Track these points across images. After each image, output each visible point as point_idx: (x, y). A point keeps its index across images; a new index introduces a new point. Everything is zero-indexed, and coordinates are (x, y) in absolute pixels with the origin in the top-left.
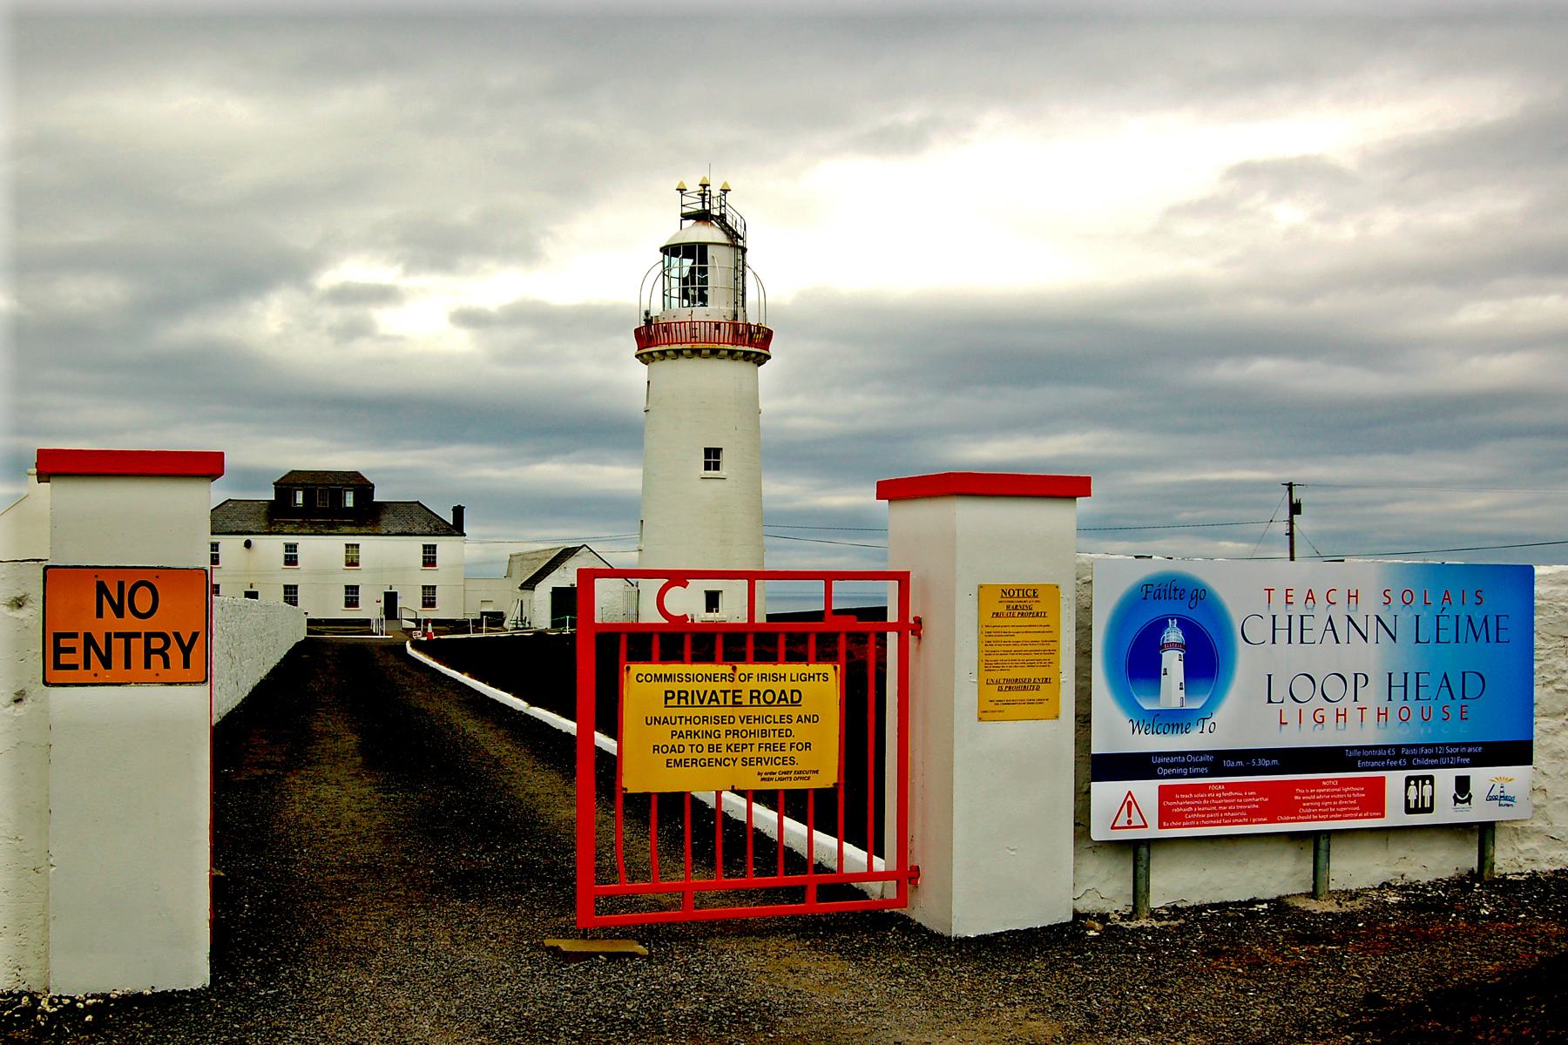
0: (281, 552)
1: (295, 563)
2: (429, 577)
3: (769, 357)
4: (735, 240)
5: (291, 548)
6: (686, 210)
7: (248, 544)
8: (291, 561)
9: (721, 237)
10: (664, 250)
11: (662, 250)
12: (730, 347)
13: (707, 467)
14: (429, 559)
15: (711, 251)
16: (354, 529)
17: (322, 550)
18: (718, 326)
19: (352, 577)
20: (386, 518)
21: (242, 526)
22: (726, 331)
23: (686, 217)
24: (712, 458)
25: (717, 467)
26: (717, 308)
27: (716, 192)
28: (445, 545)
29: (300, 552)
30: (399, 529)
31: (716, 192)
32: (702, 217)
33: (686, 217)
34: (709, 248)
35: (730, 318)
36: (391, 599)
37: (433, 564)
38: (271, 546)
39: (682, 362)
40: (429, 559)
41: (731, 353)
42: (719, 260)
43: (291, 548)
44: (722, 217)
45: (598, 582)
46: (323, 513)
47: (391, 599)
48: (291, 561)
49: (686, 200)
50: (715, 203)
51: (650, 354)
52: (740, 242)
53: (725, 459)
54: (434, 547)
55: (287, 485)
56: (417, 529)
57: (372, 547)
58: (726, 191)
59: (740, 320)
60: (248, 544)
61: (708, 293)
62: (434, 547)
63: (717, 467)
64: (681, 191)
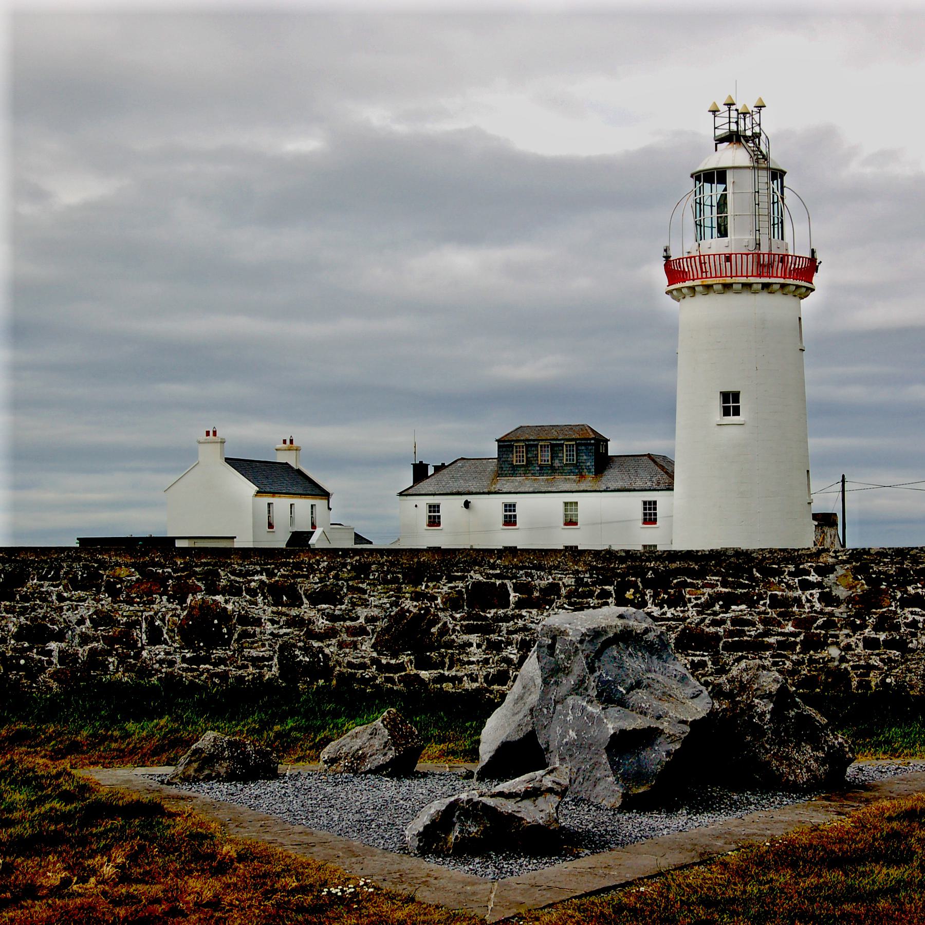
1: (439, 524)
5: (510, 507)
6: (719, 132)
7: (467, 504)
10: (697, 177)
12: (782, 281)
13: (726, 412)
14: (650, 517)
16: (575, 487)
18: (728, 258)
20: (612, 477)
21: (462, 485)
22: (749, 264)
23: (721, 140)
24: (730, 402)
25: (737, 412)
26: (739, 239)
30: (619, 485)
32: (733, 138)
33: (721, 140)
35: (752, 247)
37: (654, 521)
41: (747, 286)
43: (510, 507)
45: (176, 541)
49: (719, 121)
51: (679, 290)
53: (742, 403)
56: (639, 484)
63: (737, 412)
64: (714, 112)
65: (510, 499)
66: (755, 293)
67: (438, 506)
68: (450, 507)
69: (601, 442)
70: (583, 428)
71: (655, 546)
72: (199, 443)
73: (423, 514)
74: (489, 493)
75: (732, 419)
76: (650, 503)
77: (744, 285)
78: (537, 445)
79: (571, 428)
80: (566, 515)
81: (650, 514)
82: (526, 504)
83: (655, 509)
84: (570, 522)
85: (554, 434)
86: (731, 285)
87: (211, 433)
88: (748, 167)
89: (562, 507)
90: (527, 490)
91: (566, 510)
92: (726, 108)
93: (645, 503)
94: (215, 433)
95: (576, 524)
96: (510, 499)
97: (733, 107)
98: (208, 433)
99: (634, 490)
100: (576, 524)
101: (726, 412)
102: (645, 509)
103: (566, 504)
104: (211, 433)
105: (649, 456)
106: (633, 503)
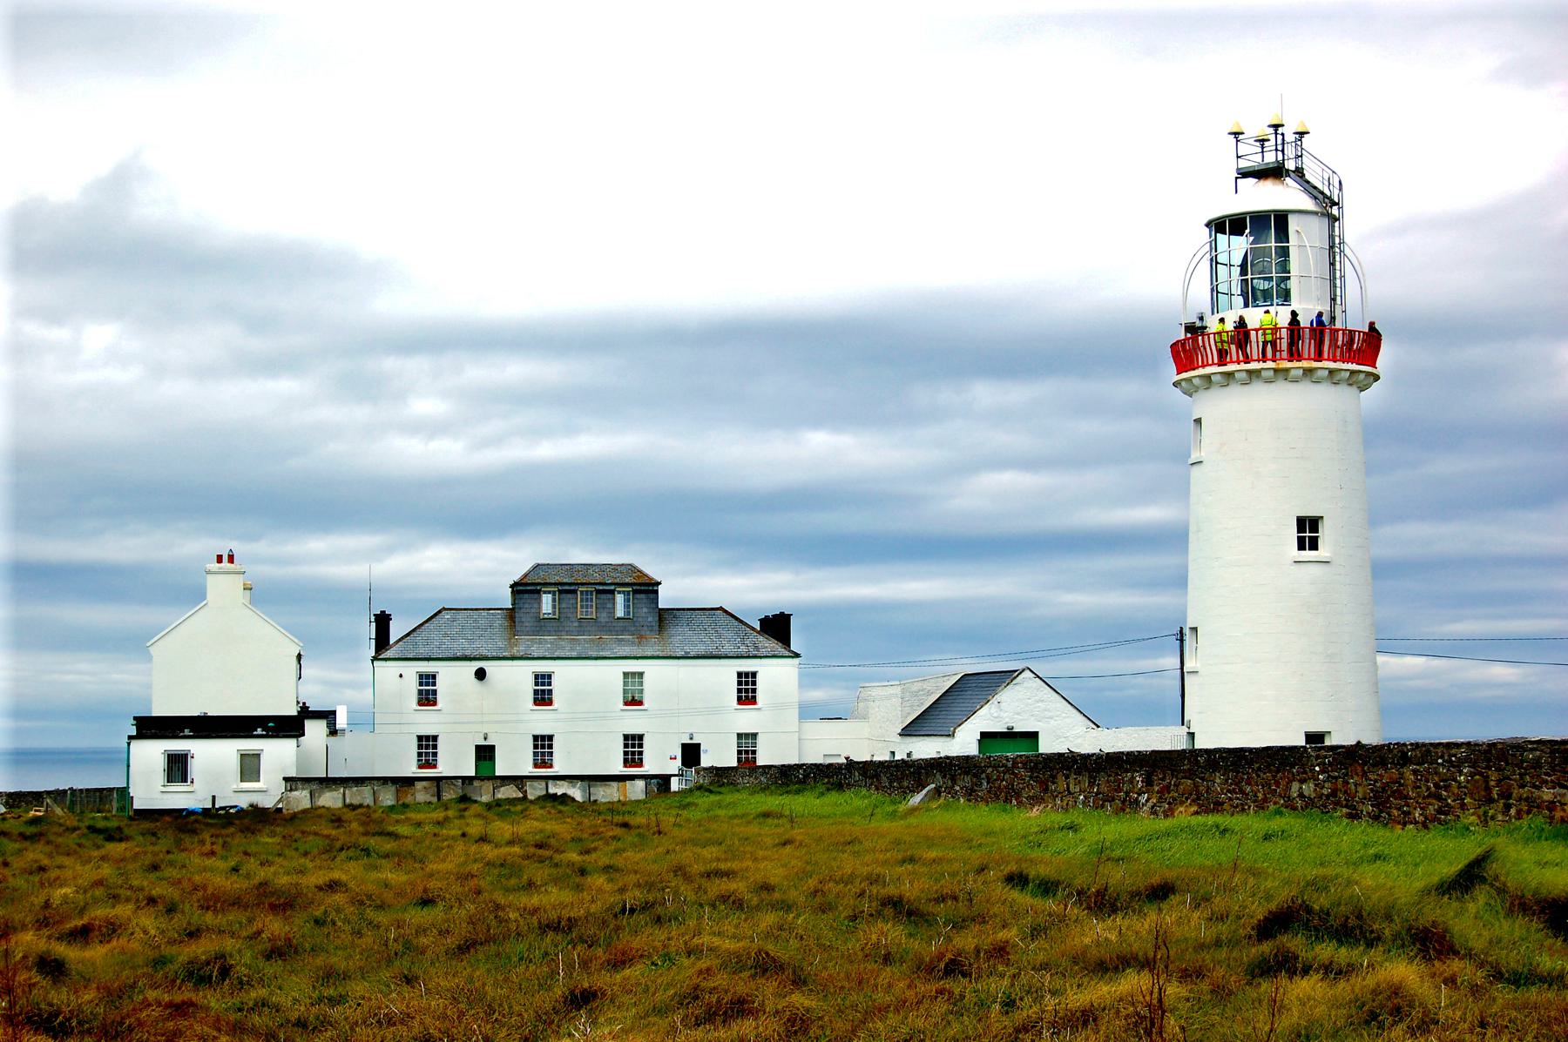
0: (529, 687)
2: (747, 719)
3: (1377, 378)
4: (1328, 206)
5: (543, 679)
6: (1243, 164)
7: (481, 674)
8: (543, 698)
9: (1308, 204)
11: (1208, 225)
13: (1301, 547)
14: (747, 691)
15: (1293, 224)
17: (589, 682)
19: (634, 722)
20: (680, 637)
21: (462, 646)
23: (1244, 174)
24: (1308, 530)
25: (1314, 545)
27: (1290, 137)
28: (775, 674)
29: (441, 686)
30: (701, 649)
31: (1290, 137)
32: (1275, 172)
33: (1244, 174)
34: (1292, 220)
36: (485, 753)
37: (753, 701)
38: (515, 677)
39: (1258, 388)
40: (747, 691)
42: (1305, 237)
43: (543, 679)
44: (1299, 172)
46: (584, 625)
47: (485, 753)
48: (543, 698)
50: (1290, 151)
52: (1335, 211)
53: (1325, 534)
54: (754, 674)
55: (525, 589)
56: (728, 648)
57: (659, 675)
58: (1302, 134)
59: (1338, 325)
60: (481, 674)
61: (1293, 285)
62: (754, 674)
63: (1314, 545)
64: (1236, 134)
65: (543, 667)
66: (1295, 381)
67: (434, 677)
68: (453, 678)
69: (646, 588)
70: (632, 568)
71: (1034, 736)
72: (209, 572)
73: (412, 687)
74: (513, 658)
75: (1308, 554)
76: (747, 675)
77: (1276, 370)
78: (574, 592)
79: (615, 568)
80: (625, 691)
81: (747, 691)
82: (568, 676)
83: (754, 683)
84: (633, 701)
85: (598, 578)
86: (1287, 370)
87: (225, 558)
88: (1316, 213)
89: (531, 680)
90: (568, 654)
91: (625, 684)
92: (1272, 130)
93: (740, 675)
94: (231, 559)
95: (640, 703)
96: (543, 667)
97: (1280, 130)
98: (220, 559)
99: (727, 657)
100: (640, 703)
101: (1301, 547)
102: (740, 683)
103: (626, 675)
104: (225, 558)
105: (721, 609)
106: (725, 674)
